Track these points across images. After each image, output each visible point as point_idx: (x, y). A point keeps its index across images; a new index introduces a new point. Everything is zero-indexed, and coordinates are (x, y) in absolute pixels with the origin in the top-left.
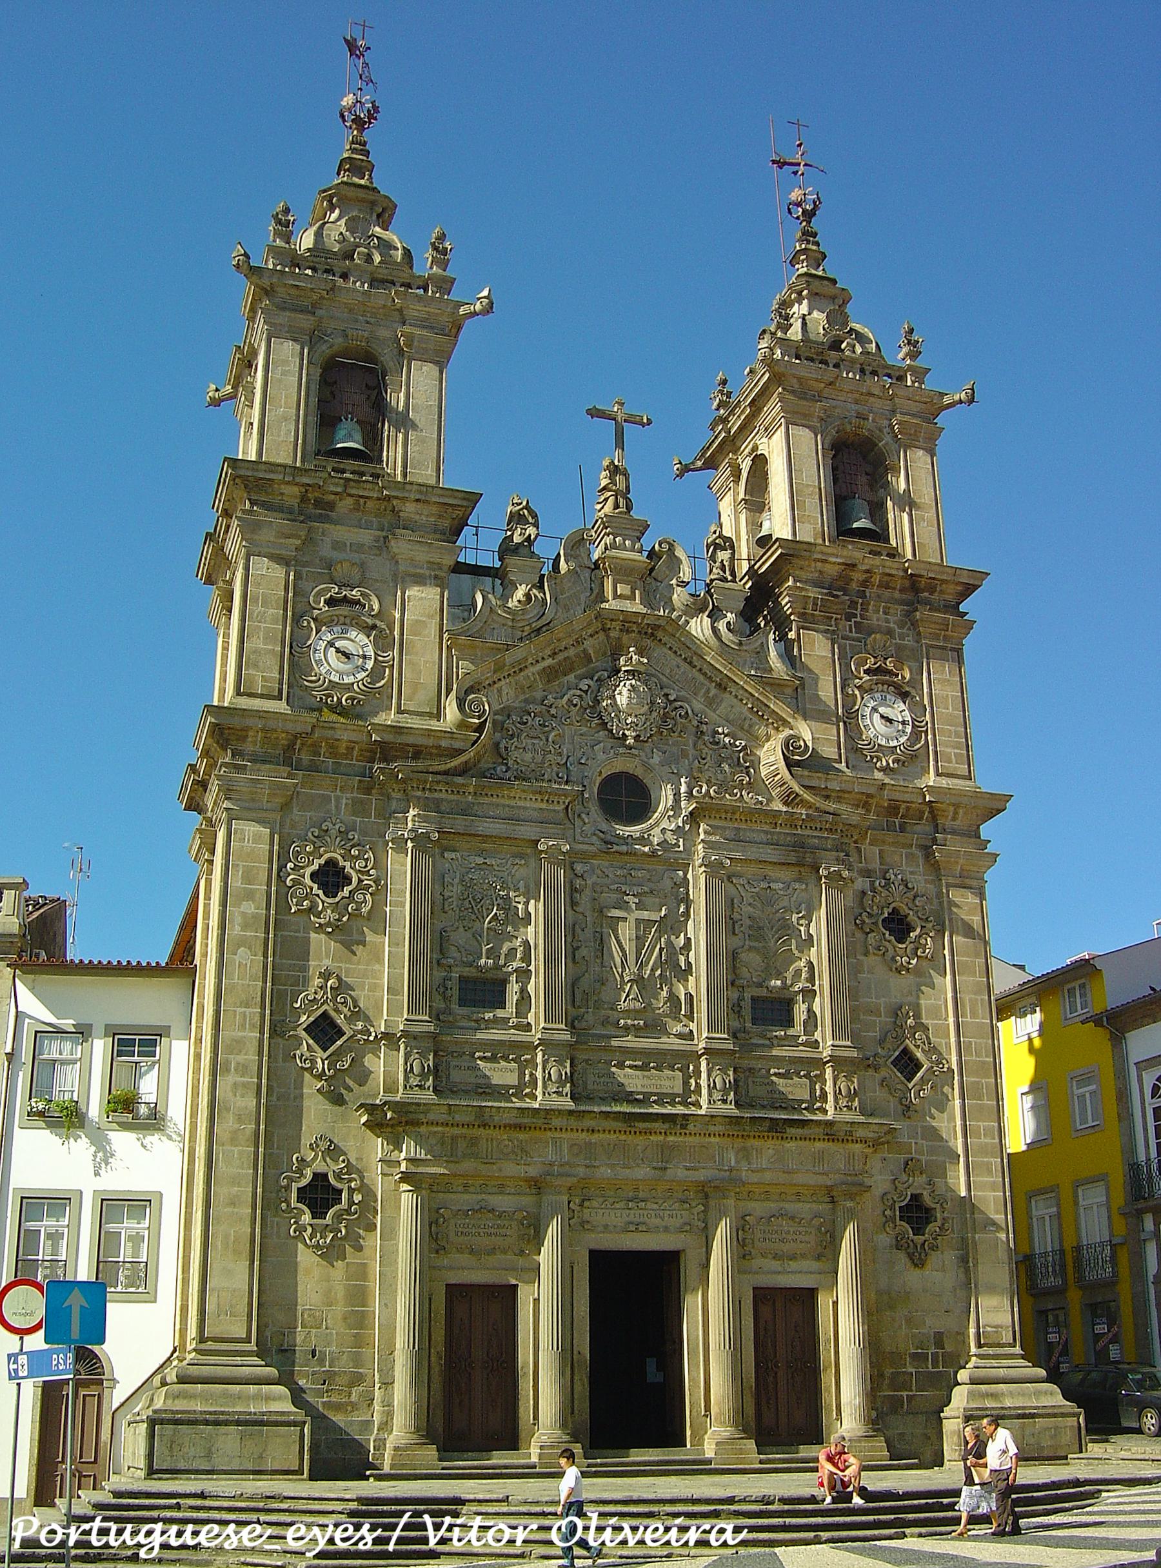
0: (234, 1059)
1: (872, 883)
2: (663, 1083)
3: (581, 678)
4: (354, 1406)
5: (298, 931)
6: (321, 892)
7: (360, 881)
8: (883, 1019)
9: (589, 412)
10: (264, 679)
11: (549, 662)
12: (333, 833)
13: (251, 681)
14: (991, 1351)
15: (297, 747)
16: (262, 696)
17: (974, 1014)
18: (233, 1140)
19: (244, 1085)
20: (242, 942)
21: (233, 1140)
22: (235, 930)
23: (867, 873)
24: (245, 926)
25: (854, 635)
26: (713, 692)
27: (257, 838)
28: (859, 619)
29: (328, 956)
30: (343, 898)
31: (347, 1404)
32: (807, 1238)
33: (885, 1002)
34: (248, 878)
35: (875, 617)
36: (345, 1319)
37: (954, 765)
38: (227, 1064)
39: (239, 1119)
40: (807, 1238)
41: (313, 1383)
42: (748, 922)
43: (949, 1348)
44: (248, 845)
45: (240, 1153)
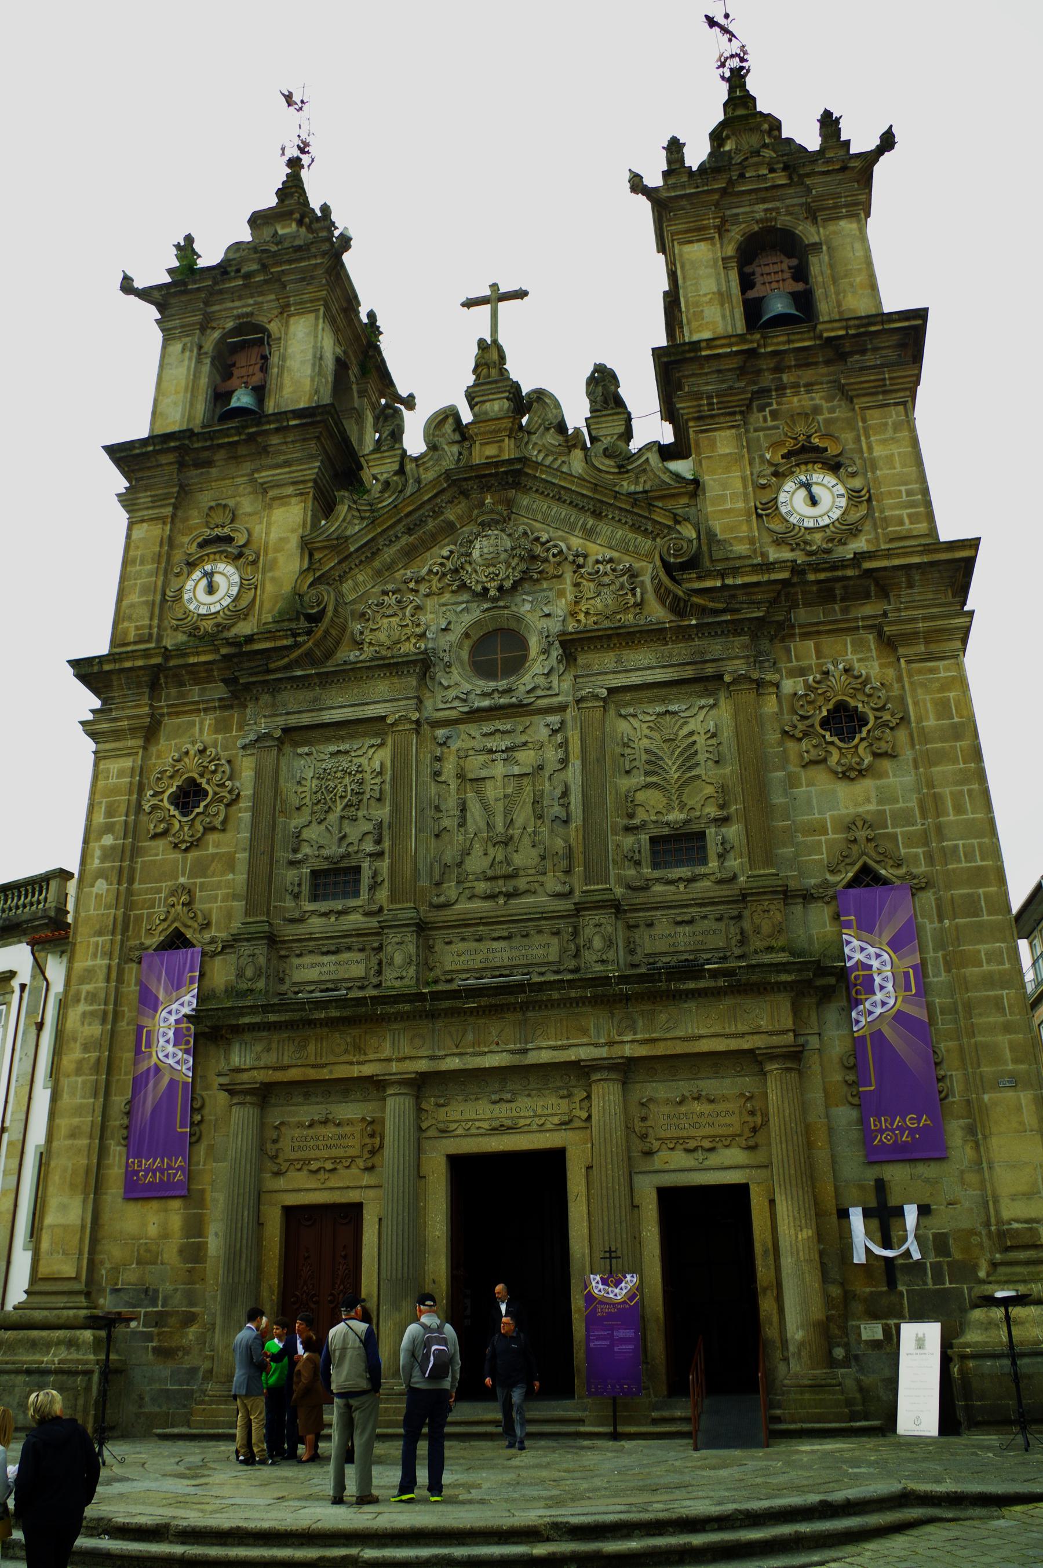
0: (86, 988)
1: (806, 682)
2: (535, 952)
3: (441, 548)
4: (187, 1351)
5: (157, 855)
6: (176, 813)
7: (215, 794)
8: (831, 836)
9: (463, 305)
10: (137, 628)
11: (405, 540)
12: (192, 752)
13: (125, 633)
14: (1022, 1255)
15: (162, 681)
16: (135, 643)
17: (959, 809)
18: (78, 1071)
19: (92, 1014)
20: (101, 874)
21: (78, 1071)
22: (95, 863)
23: (802, 672)
24: (104, 858)
25: (770, 423)
26: (591, 522)
27: (121, 774)
28: (775, 406)
29: (183, 875)
30: (198, 814)
31: (178, 1349)
32: (728, 1120)
33: (832, 817)
34: (109, 814)
35: (795, 399)
36: (181, 1252)
37: (907, 525)
38: (78, 994)
39: (86, 1048)
40: (728, 1120)
41: (144, 1326)
42: (644, 757)
43: (957, 1255)
44: (113, 781)
45: (84, 1083)
